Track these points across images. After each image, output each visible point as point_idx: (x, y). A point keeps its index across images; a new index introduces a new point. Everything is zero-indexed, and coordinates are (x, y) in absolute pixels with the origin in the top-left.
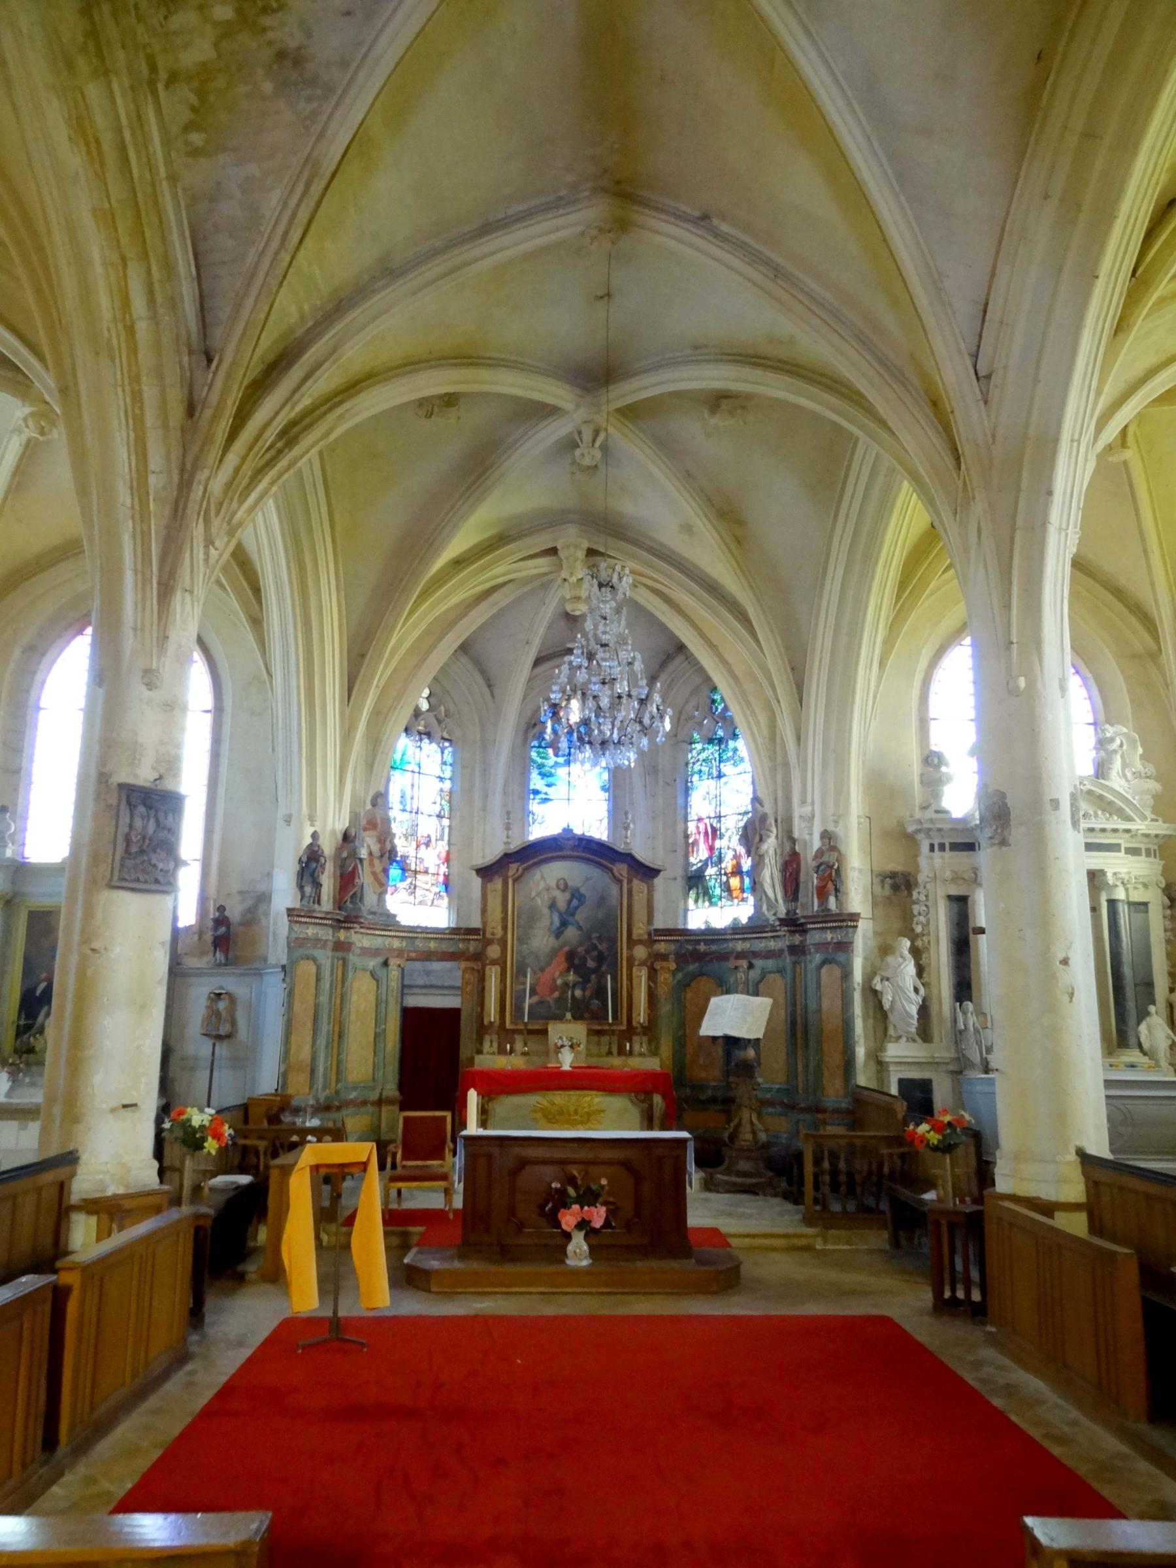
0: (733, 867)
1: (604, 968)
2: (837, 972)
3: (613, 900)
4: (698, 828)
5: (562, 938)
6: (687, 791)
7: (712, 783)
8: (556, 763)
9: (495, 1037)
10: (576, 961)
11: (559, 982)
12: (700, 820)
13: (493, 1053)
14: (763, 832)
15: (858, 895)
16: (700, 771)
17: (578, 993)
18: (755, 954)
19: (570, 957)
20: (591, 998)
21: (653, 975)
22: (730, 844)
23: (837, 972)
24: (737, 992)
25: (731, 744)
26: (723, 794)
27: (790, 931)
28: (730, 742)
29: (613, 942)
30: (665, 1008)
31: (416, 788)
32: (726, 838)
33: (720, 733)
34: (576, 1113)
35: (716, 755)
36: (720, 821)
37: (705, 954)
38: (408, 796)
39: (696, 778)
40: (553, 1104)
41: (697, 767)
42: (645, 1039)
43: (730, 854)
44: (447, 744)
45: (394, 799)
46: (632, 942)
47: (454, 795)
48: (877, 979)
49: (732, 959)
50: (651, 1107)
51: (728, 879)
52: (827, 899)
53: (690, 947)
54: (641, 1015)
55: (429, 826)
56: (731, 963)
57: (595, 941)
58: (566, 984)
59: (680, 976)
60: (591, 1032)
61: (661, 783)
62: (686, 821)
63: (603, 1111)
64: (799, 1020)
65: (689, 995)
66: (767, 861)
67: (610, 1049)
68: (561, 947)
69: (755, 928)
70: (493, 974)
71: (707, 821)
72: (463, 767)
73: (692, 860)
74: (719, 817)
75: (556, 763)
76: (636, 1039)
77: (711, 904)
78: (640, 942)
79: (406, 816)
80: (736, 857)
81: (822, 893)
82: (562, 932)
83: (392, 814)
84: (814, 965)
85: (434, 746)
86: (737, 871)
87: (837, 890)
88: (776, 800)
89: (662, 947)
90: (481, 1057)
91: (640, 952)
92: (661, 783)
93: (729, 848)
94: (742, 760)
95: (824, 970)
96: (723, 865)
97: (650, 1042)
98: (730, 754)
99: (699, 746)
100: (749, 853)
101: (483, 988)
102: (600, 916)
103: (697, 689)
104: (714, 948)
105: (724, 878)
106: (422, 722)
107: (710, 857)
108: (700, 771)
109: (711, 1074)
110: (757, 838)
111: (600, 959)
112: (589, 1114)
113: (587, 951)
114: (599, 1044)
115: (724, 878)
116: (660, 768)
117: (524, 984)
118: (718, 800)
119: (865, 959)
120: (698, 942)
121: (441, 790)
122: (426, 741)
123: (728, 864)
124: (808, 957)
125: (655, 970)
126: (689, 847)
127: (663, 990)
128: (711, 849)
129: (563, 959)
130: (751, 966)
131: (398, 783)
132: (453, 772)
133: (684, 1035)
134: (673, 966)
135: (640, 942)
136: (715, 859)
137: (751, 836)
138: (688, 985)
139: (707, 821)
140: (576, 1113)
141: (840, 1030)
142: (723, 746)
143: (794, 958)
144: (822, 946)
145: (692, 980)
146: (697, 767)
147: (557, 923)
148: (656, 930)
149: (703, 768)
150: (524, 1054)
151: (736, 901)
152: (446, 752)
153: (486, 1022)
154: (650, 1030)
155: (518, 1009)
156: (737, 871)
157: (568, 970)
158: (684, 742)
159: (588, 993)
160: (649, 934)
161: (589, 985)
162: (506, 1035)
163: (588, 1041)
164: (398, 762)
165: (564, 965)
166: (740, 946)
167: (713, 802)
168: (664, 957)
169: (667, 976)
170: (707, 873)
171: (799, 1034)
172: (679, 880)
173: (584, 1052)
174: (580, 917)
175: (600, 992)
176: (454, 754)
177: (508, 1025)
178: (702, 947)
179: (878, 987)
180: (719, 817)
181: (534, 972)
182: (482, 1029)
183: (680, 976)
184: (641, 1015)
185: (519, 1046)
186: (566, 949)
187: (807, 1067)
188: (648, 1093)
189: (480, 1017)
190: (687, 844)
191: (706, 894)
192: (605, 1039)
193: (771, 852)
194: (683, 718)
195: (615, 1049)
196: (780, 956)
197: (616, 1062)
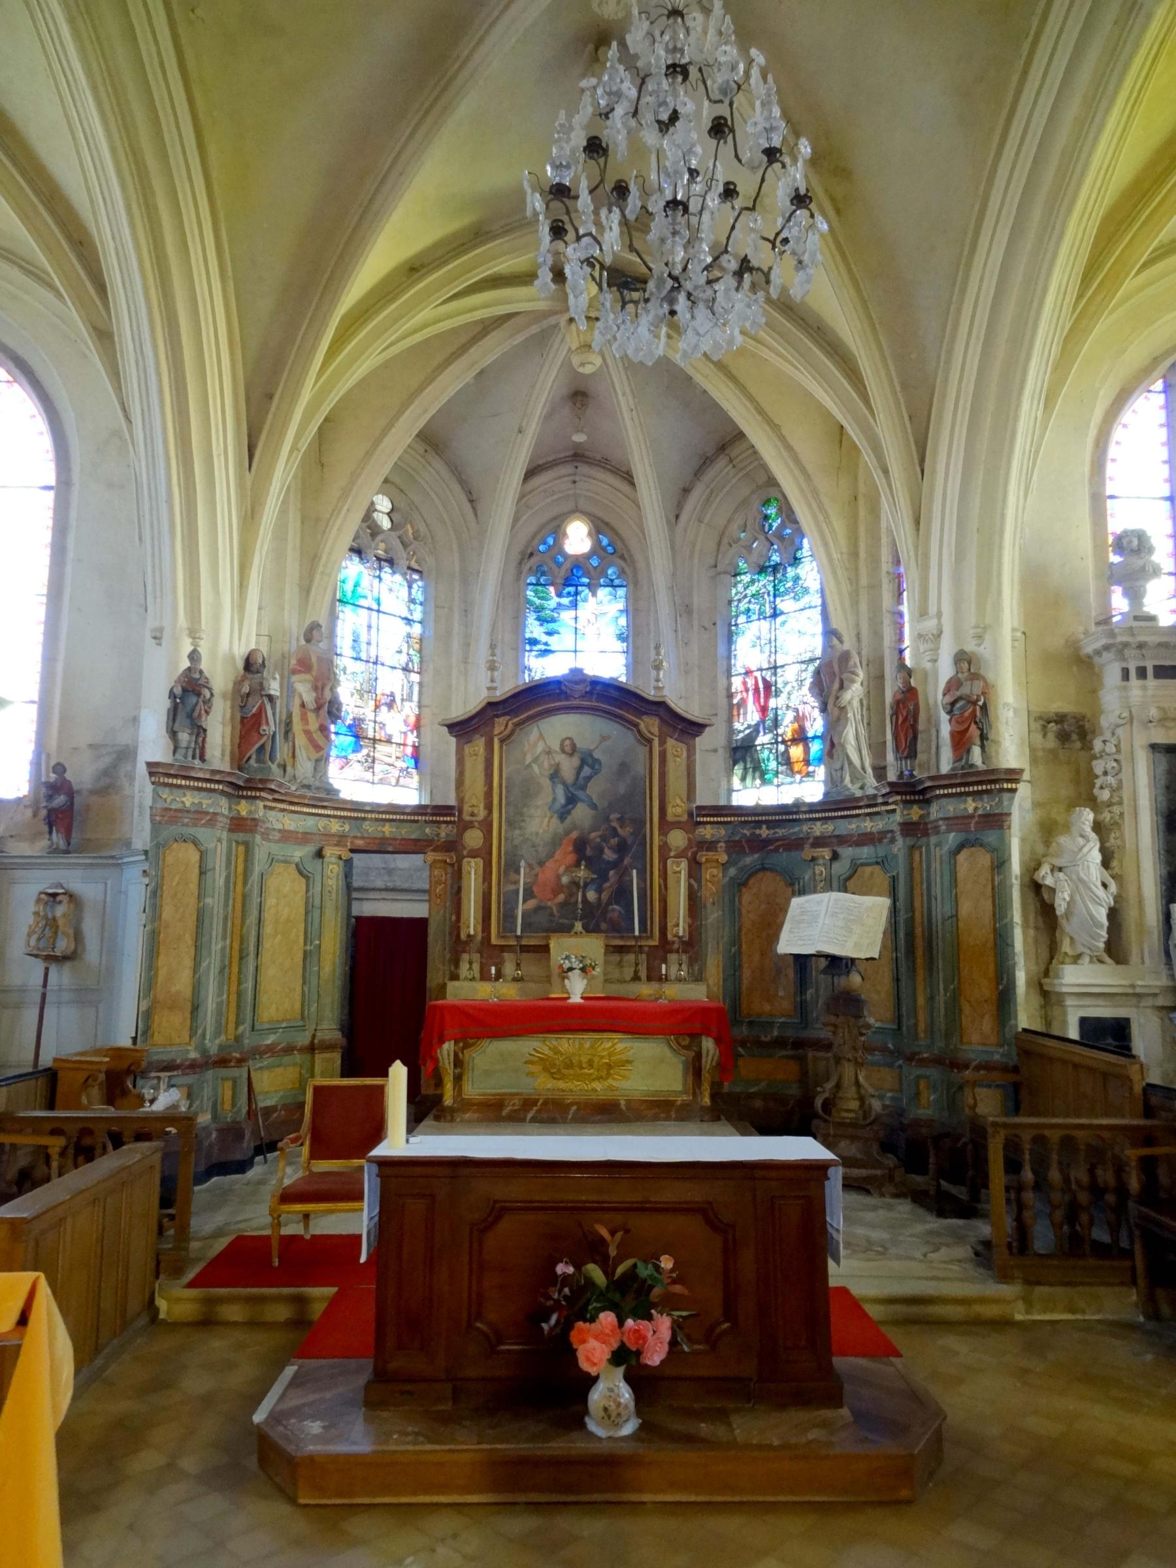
0: (794, 731)
1: (627, 861)
2: (984, 859)
3: (640, 769)
4: (745, 683)
5: (569, 820)
6: (730, 639)
7: (765, 624)
8: (559, 604)
9: (476, 957)
10: (589, 852)
11: (565, 880)
12: (748, 673)
13: (473, 979)
14: (844, 676)
15: (1011, 745)
16: (748, 610)
17: (591, 895)
18: (843, 840)
19: (580, 846)
20: (609, 903)
21: (695, 868)
22: (797, 699)
23: (984, 859)
24: (815, 892)
25: (791, 572)
26: (780, 640)
27: (905, 802)
28: (789, 569)
29: (639, 824)
30: (713, 916)
31: (374, 631)
32: (784, 696)
33: (776, 558)
34: (590, 1064)
35: (770, 588)
36: (775, 674)
37: (767, 842)
38: (364, 638)
39: (742, 619)
40: (556, 1051)
41: (743, 606)
42: (684, 957)
43: (790, 715)
44: (416, 577)
45: (344, 643)
46: (666, 826)
47: (425, 643)
48: (1045, 869)
49: (807, 846)
50: (699, 1056)
51: (787, 747)
52: (968, 751)
53: (747, 832)
54: (679, 925)
55: (391, 682)
56: (808, 852)
57: (615, 824)
58: (575, 883)
59: (732, 871)
60: (612, 950)
61: (696, 628)
62: (729, 675)
63: (629, 1062)
64: (918, 931)
65: (747, 897)
66: (850, 715)
67: (636, 972)
68: (568, 833)
69: (836, 805)
70: (472, 870)
71: (758, 674)
72: (437, 607)
73: (737, 726)
74: (774, 668)
75: (559, 604)
76: (673, 957)
77: (764, 782)
78: (677, 825)
79: (360, 666)
80: (799, 719)
81: (960, 742)
82: (569, 812)
83: (340, 662)
84: (946, 848)
85: (398, 578)
86: (801, 737)
87: (983, 737)
88: (858, 635)
89: (707, 832)
90: (456, 983)
91: (677, 839)
92: (696, 628)
93: (788, 707)
94: (806, 591)
95: (962, 857)
96: (780, 731)
97: (692, 962)
98: (789, 584)
99: (746, 578)
100: (824, 709)
101: (459, 890)
102: (622, 789)
103: (745, 502)
104: (781, 832)
105: (782, 748)
106: (382, 546)
107: (763, 721)
108: (748, 610)
109: (778, 1005)
110: (836, 685)
111: (622, 848)
112: (609, 1066)
113: (604, 838)
114: (620, 964)
115: (782, 748)
116: (695, 607)
117: (517, 882)
118: (773, 645)
119: (1023, 840)
120: (759, 824)
121: (409, 636)
122: (388, 570)
123: (787, 729)
124: (933, 839)
125: (699, 864)
126: (733, 709)
127: (709, 892)
128: (764, 710)
129: (571, 848)
130: (835, 857)
131: (349, 623)
132: (424, 613)
133: (740, 952)
134: (724, 858)
135: (677, 825)
136: (768, 723)
137: (828, 681)
138: (744, 884)
139: (758, 674)
140: (590, 1064)
141: (990, 944)
142: (779, 576)
143: (910, 841)
144: (959, 822)
145: (750, 876)
146: (743, 606)
147: (562, 800)
148: (698, 808)
149: (751, 606)
150: (516, 980)
151: (798, 777)
152: (415, 586)
153: (463, 936)
154: (692, 946)
155: (508, 917)
156: (801, 737)
157: (577, 864)
158: (725, 573)
159: (605, 896)
160: (690, 815)
161: (607, 885)
162: (491, 953)
163: (606, 962)
164: (349, 594)
165: (571, 858)
166: (818, 829)
168: (711, 846)
169: (715, 871)
171: (919, 952)
172: (721, 751)
173: (601, 979)
174: (595, 789)
175: (622, 894)
176: (425, 590)
177: (494, 940)
178: (764, 832)
179: (1049, 881)
180: (774, 668)
181: (530, 866)
182: (458, 945)
183: (732, 871)
184: (679, 925)
185: (509, 969)
186: (574, 835)
187: (931, 999)
188: (695, 1036)
189: (456, 927)
190: (731, 706)
191: (757, 770)
192: (631, 957)
193: (856, 703)
194: (725, 541)
195: (643, 974)
196: (880, 840)
197: (646, 990)
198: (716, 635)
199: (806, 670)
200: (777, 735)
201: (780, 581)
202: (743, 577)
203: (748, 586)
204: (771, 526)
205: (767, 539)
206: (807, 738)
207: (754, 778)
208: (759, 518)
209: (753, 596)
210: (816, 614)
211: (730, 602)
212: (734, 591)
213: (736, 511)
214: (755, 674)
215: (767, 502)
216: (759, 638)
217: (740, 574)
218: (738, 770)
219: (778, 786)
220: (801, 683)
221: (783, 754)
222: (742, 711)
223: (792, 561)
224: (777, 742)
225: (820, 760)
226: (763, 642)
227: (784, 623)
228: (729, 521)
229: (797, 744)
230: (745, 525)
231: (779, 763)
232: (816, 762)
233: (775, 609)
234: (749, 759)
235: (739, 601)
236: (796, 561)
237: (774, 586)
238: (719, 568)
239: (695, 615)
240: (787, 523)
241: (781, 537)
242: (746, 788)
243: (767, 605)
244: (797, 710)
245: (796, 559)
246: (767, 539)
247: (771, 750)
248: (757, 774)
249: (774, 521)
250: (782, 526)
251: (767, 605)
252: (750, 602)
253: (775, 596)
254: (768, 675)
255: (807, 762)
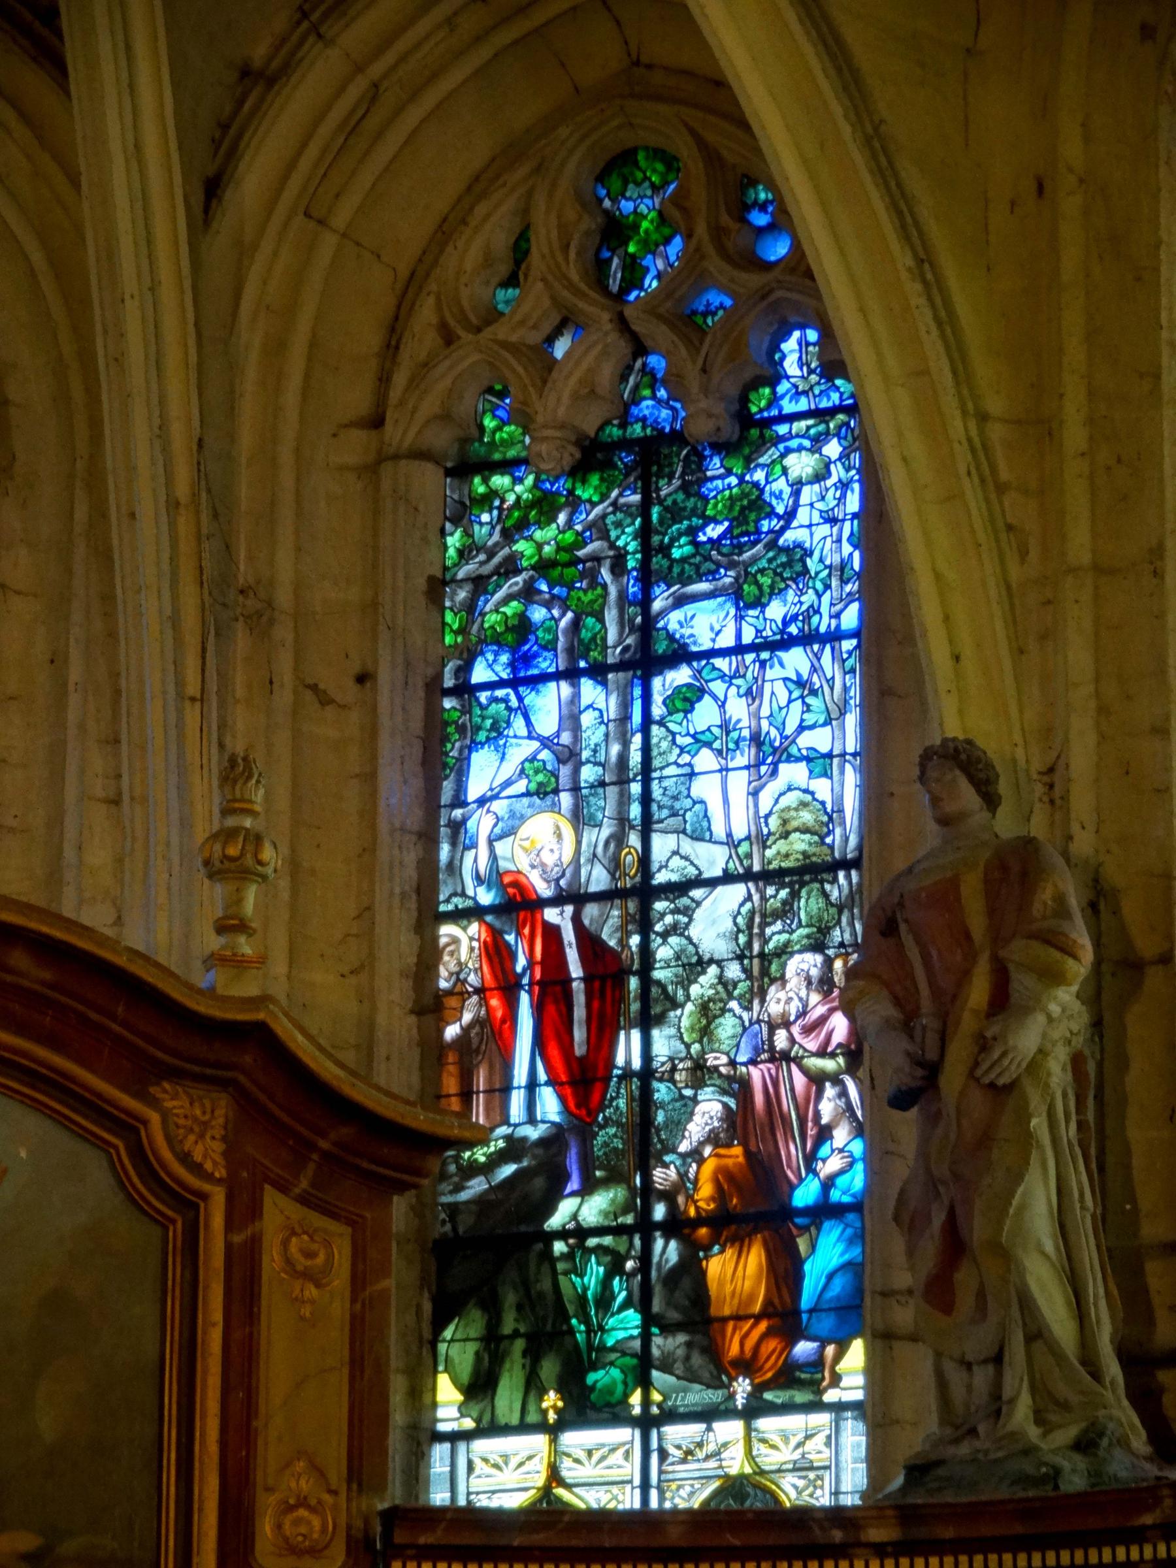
0: (725, 1180)
12: (518, 903)
16: (522, 627)
25: (722, 480)
28: (715, 466)
35: (627, 540)
36: (645, 925)
41: (498, 610)
43: (710, 1108)
62: (429, 917)
74: (640, 893)
80: (751, 1124)
86: (757, 1207)
93: (700, 1072)
94: (793, 565)
96: (663, 1176)
108: (522, 627)
116: (284, 597)
118: (637, 797)
128: (584, 1080)
136: (607, 1137)
146: (498, 610)
149: (538, 614)
158: (422, 455)
167: (606, 805)
170: (556, 1221)
198: (372, 732)
199: (786, 911)
200: (648, 1192)
201: (674, 513)
202: (500, 481)
203: (530, 519)
204: (634, 273)
205: (622, 324)
206: (788, 1212)
207: (533, 1386)
208: (590, 223)
209: (543, 567)
210: (838, 672)
211: (438, 586)
212: (454, 541)
213: (477, 187)
214: (551, 915)
215: (618, 166)
216: (570, 756)
217: (489, 467)
218: (458, 1346)
219: (646, 1423)
220: (764, 969)
221: (673, 1278)
222: (481, 1080)
223: (730, 430)
224: (645, 1227)
225: (849, 1314)
226: (588, 774)
227: (686, 699)
228: (445, 232)
229: (740, 1241)
230: (520, 250)
231: (649, 1320)
232: (825, 1324)
233: (647, 627)
234: (510, 1299)
235: (480, 584)
236: (749, 434)
237: (645, 534)
238: (396, 434)
239: (284, 632)
240: (714, 264)
241: (688, 325)
242: (490, 1428)
243: (611, 616)
244: (740, 1088)
245: (745, 420)
246: (622, 324)
247: (615, 1267)
248: (549, 1368)
249: (650, 247)
250: (690, 276)
251: (611, 616)
252: (528, 594)
253: (647, 578)
254: (609, 926)
255: (785, 1318)
